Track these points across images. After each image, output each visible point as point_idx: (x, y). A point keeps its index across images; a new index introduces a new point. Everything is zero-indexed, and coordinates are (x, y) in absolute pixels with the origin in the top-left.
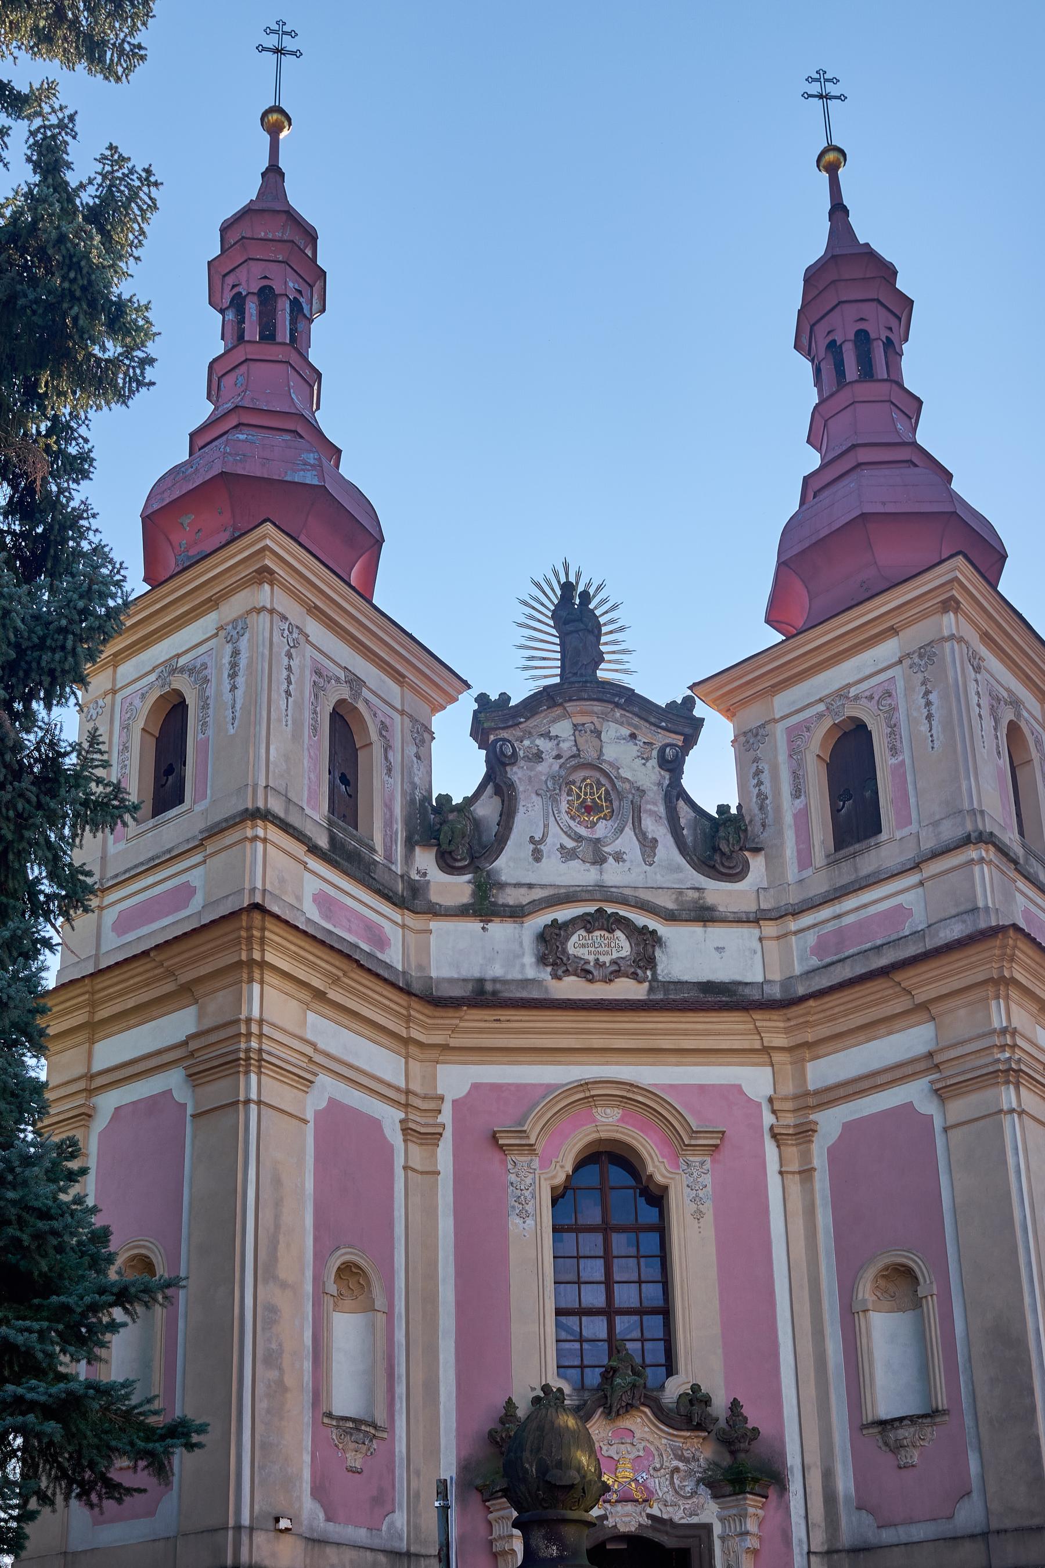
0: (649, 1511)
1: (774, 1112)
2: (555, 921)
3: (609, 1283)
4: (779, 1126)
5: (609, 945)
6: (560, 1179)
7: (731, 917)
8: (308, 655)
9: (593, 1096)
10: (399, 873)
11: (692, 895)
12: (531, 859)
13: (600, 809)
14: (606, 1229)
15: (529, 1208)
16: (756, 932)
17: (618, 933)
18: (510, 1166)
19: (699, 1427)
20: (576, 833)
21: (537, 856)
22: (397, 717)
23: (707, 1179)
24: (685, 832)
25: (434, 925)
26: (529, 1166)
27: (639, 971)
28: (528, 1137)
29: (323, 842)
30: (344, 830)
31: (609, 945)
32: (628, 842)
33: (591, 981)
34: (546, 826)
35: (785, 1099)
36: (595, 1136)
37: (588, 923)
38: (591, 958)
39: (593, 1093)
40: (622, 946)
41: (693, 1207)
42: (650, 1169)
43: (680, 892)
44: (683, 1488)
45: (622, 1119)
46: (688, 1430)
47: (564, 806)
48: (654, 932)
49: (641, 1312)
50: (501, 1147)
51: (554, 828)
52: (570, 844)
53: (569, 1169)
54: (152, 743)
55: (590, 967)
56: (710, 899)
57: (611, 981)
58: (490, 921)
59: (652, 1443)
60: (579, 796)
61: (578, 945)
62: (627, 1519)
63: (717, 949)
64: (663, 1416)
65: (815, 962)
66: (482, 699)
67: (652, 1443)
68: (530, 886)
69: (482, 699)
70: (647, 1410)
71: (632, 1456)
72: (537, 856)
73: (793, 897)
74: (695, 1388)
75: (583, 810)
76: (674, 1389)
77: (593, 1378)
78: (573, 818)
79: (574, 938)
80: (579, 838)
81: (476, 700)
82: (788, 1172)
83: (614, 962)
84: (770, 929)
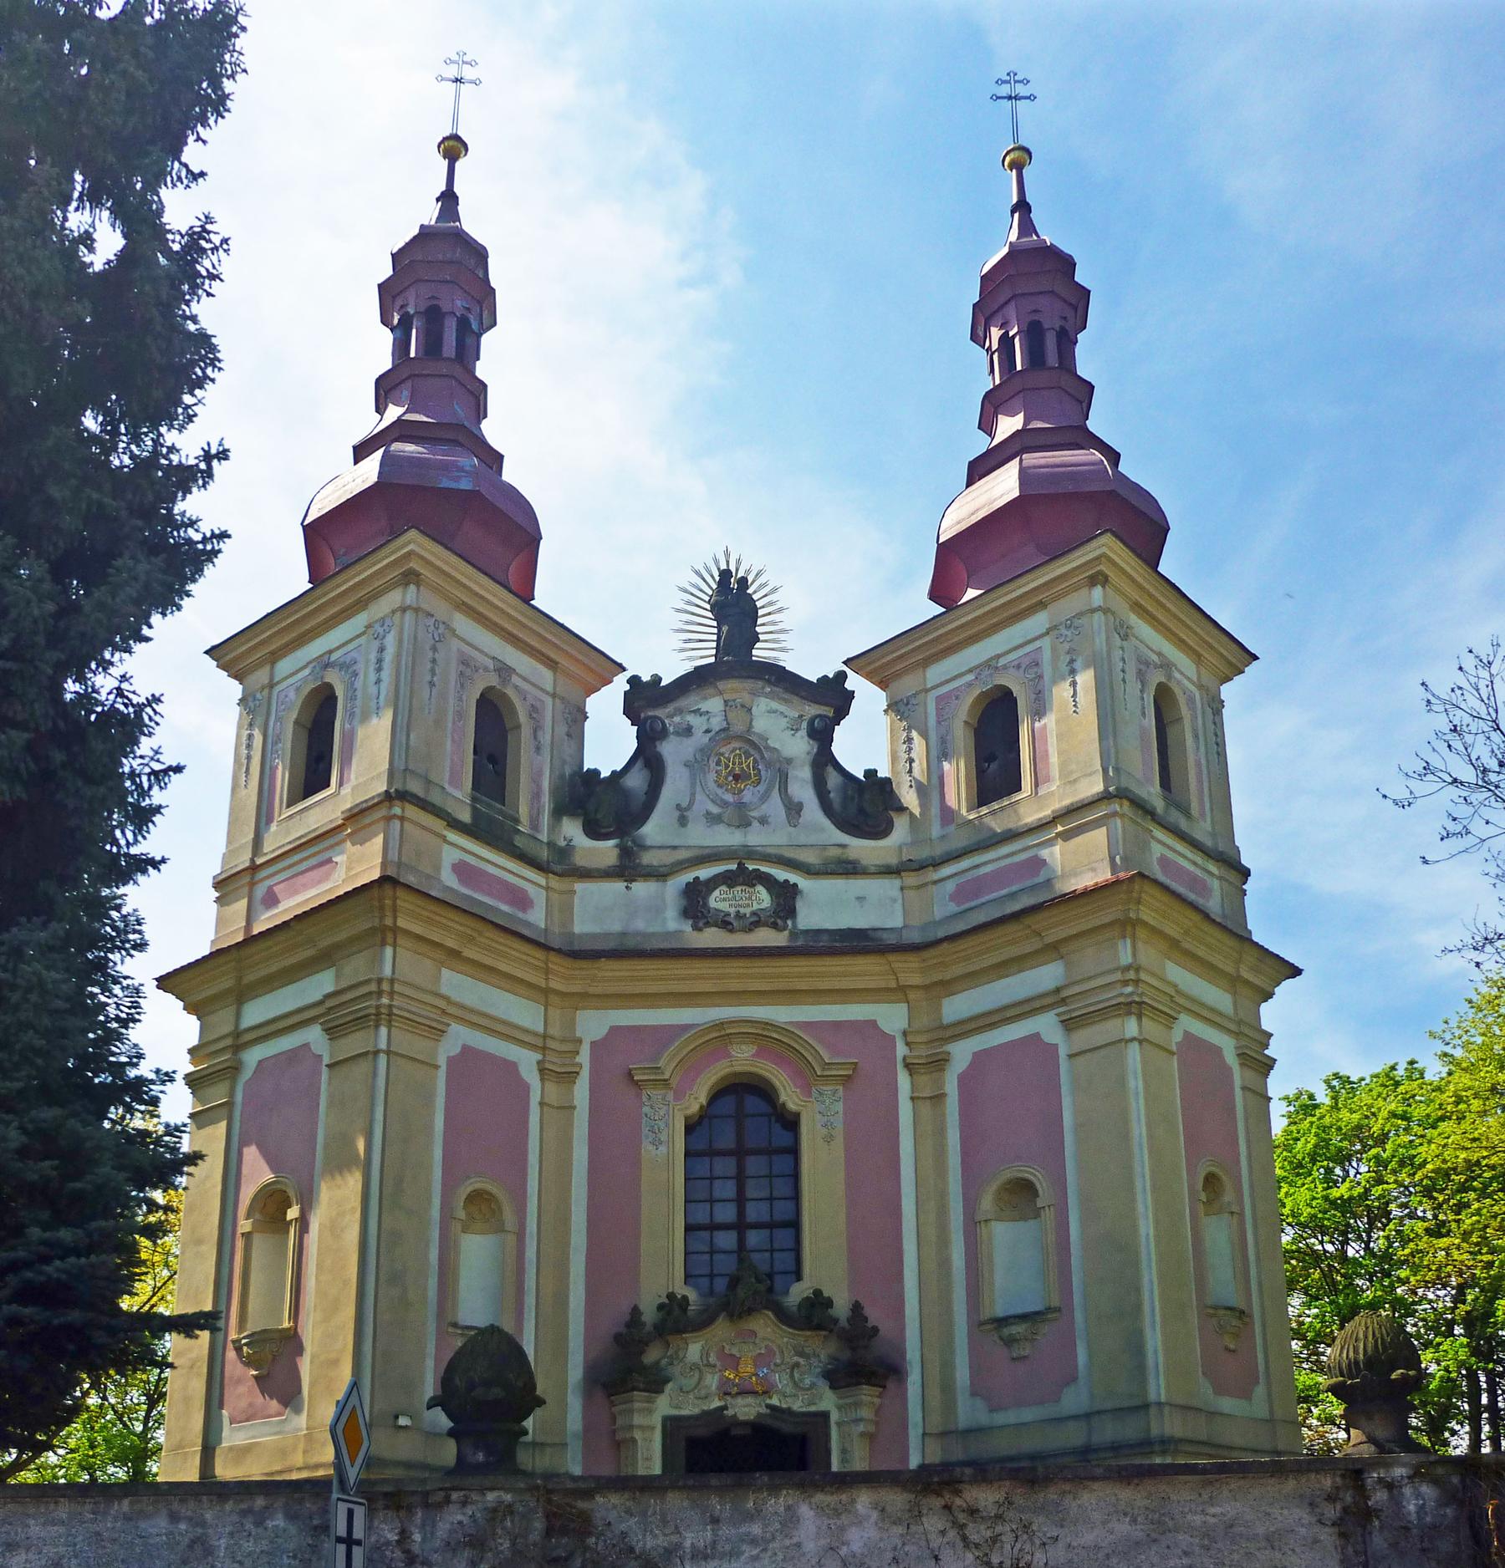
0: (768, 1401)
1: (907, 1044)
2: (697, 878)
3: (741, 1200)
4: (910, 1057)
5: (750, 898)
6: (694, 1108)
7: (873, 869)
8: (454, 648)
9: (728, 1035)
10: (545, 840)
11: (834, 852)
12: (676, 825)
13: (748, 777)
14: (740, 1153)
15: (663, 1138)
16: (897, 883)
17: (760, 888)
18: (644, 1099)
19: (819, 1327)
20: (722, 800)
21: (683, 821)
22: (549, 701)
23: (839, 1107)
24: (832, 795)
25: (579, 887)
26: (664, 1099)
27: (779, 921)
28: (663, 1073)
29: (465, 816)
30: (489, 806)
31: (750, 898)
32: (775, 807)
33: (731, 931)
34: (693, 795)
35: (918, 1032)
36: (728, 1070)
37: (728, 879)
38: (732, 910)
39: (728, 1031)
40: (762, 898)
41: (824, 1131)
42: (783, 1098)
43: (824, 847)
44: (801, 1380)
45: (757, 1055)
46: (809, 1329)
47: (712, 776)
48: (795, 885)
49: (771, 1226)
50: (636, 1083)
51: (699, 797)
52: (715, 810)
53: (703, 1100)
54: (304, 736)
55: (731, 919)
56: (852, 854)
57: (750, 930)
58: (635, 881)
59: (773, 1342)
60: (727, 766)
61: (718, 900)
62: (746, 1409)
63: (858, 898)
64: (784, 1317)
65: (953, 908)
66: (634, 681)
67: (773, 1342)
68: (675, 848)
69: (634, 681)
70: (770, 1313)
71: (754, 1354)
72: (683, 821)
73: (939, 851)
74: (818, 1293)
75: (731, 778)
76: (797, 1293)
77: (721, 1284)
78: (720, 786)
79: (716, 893)
80: (725, 804)
81: (628, 682)
82: (918, 1098)
83: (754, 913)
84: (911, 879)
